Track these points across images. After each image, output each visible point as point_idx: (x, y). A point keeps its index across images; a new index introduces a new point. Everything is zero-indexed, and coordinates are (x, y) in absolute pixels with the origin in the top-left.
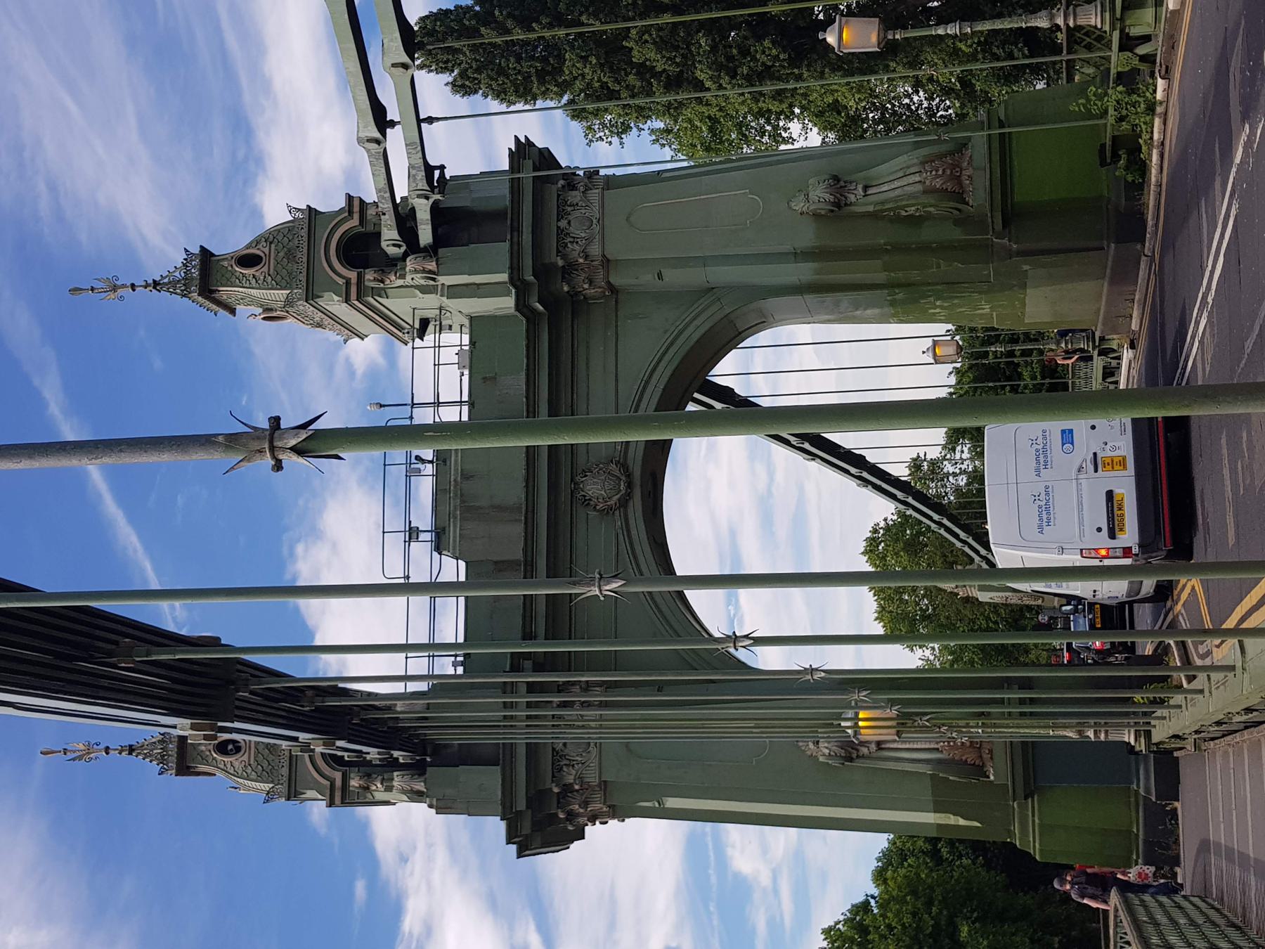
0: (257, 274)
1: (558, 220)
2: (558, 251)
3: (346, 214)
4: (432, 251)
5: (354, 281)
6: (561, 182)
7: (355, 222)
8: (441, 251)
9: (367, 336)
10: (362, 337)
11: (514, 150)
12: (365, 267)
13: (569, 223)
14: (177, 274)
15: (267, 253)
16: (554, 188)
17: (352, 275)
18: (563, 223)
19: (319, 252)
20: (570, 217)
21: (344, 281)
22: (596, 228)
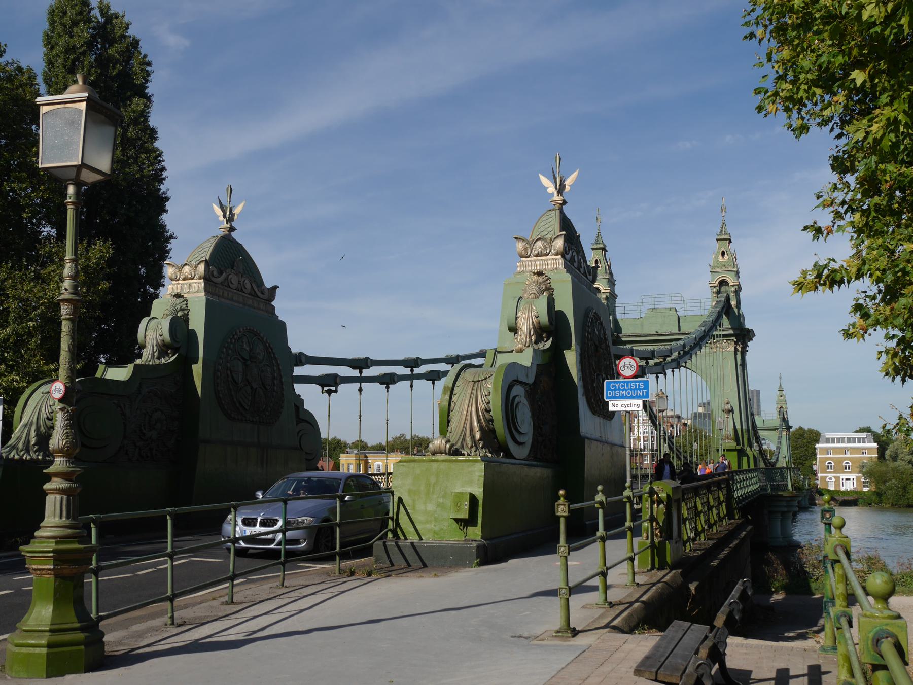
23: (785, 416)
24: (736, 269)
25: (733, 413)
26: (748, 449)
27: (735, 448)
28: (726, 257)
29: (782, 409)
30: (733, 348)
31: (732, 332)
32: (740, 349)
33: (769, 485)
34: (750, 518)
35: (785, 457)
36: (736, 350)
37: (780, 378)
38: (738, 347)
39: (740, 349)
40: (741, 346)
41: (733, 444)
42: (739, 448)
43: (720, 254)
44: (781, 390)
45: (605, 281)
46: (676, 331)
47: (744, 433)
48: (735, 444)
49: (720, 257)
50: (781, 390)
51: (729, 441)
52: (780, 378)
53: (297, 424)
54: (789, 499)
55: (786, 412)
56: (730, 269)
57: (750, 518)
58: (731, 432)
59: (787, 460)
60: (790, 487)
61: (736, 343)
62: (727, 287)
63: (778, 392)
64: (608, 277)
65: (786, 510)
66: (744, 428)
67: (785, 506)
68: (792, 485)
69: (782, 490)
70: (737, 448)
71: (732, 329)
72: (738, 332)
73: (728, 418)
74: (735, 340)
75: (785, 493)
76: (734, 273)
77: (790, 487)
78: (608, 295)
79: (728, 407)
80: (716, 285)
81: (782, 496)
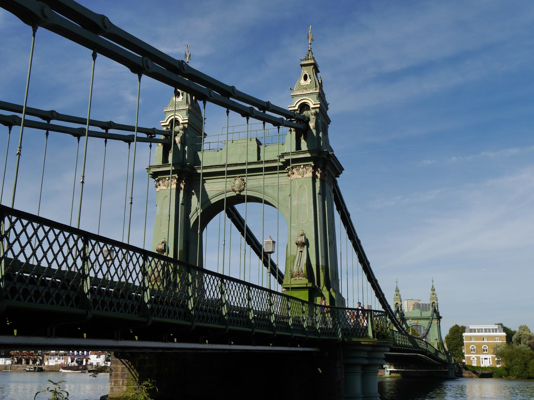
23: (436, 309)
24: (318, 91)
25: (308, 247)
26: (325, 288)
27: (305, 286)
28: (309, 80)
29: (434, 304)
30: (310, 174)
31: (308, 155)
32: (319, 175)
33: (340, 329)
34: (321, 371)
35: (437, 340)
36: (314, 178)
37: (433, 281)
38: (317, 173)
39: (319, 175)
40: (320, 172)
41: (304, 281)
42: (310, 285)
43: (303, 78)
44: (433, 290)
45: (185, 112)
46: (255, 159)
47: (321, 271)
48: (306, 281)
49: (302, 82)
50: (433, 290)
51: (301, 278)
52: (433, 281)
53: (70, 307)
54: (370, 349)
55: (437, 306)
56: (311, 91)
57: (321, 371)
58: (304, 268)
59: (438, 342)
60: (370, 334)
61: (315, 168)
62: (309, 112)
63: (431, 291)
64: (188, 108)
65: (366, 362)
66: (320, 264)
67: (367, 358)
68: (373, 332)
69: (359, 337)
70: (308, 286)
71: (309, 151)
72: (315, 155)
73: (302, 252)
74: (313, 165)
75: (363, 341)
76: (315, 96)
77: (370, 334)
78: (186, 125)
79: (302, 239)
80: (296, 108)
81: (359, 344)
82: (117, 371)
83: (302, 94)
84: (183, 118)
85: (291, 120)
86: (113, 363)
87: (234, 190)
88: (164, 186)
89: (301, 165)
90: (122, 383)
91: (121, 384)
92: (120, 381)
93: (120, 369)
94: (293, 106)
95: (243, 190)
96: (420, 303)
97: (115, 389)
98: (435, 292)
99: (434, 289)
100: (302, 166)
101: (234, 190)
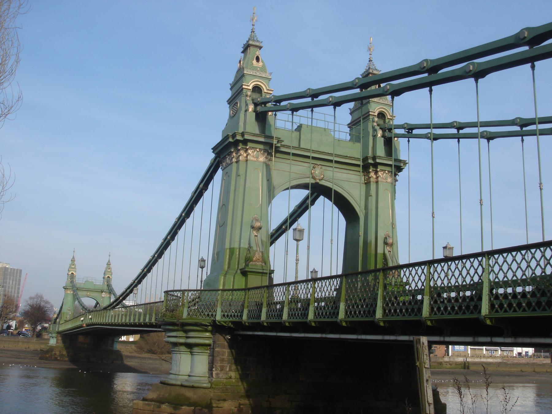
0: (254, 61)
1: (259, 149)
2: (250, 147)
3: (268, 89)
4: (255, 111)
5: (248, 88)
6: (270, 151)
7: (266, 91)
8: (255, 113)
9: (231, 90)
10: (231, 89)
11: (281, 139)
12: (252, 92)
13: (258, 152)
14: (256, 38)
15: (259, 65)
16: (268, 149)
17: (251, 87)
18: (258, 150)
19: (258, 79)
20: (259, 152)
21: (249, 85)
22: (255, 159)
37: (110, 256)
44: (109, 264)
50: (109, 264)
52: (110, 256)
82: (223, 355)
83: (378, 102)
84: (269, 88)
85: (409, 131)
86: (218, 347)
87: (314, 178)
88: (253, 156)
89: (386, 171)
90: (229, 369)
91: (228, 370)
92: (227, 366)
93: (227, 353)
94: (374, 111)
95: (322, 179)
96: (7, 267)
97: (221, 375)
98: (111, 266)
99: (109, 264)
100: (387, 172)
101: (314, 178)
